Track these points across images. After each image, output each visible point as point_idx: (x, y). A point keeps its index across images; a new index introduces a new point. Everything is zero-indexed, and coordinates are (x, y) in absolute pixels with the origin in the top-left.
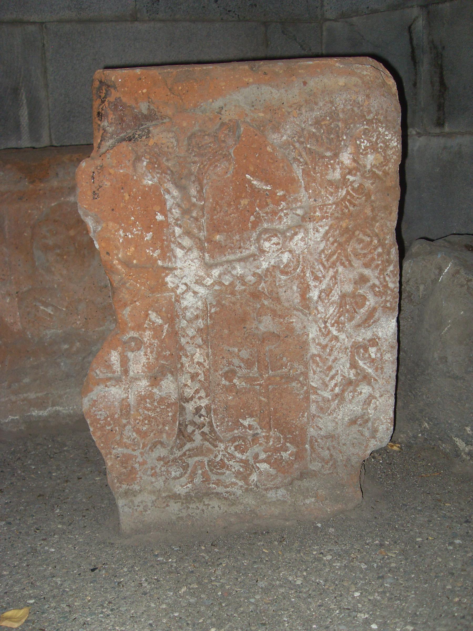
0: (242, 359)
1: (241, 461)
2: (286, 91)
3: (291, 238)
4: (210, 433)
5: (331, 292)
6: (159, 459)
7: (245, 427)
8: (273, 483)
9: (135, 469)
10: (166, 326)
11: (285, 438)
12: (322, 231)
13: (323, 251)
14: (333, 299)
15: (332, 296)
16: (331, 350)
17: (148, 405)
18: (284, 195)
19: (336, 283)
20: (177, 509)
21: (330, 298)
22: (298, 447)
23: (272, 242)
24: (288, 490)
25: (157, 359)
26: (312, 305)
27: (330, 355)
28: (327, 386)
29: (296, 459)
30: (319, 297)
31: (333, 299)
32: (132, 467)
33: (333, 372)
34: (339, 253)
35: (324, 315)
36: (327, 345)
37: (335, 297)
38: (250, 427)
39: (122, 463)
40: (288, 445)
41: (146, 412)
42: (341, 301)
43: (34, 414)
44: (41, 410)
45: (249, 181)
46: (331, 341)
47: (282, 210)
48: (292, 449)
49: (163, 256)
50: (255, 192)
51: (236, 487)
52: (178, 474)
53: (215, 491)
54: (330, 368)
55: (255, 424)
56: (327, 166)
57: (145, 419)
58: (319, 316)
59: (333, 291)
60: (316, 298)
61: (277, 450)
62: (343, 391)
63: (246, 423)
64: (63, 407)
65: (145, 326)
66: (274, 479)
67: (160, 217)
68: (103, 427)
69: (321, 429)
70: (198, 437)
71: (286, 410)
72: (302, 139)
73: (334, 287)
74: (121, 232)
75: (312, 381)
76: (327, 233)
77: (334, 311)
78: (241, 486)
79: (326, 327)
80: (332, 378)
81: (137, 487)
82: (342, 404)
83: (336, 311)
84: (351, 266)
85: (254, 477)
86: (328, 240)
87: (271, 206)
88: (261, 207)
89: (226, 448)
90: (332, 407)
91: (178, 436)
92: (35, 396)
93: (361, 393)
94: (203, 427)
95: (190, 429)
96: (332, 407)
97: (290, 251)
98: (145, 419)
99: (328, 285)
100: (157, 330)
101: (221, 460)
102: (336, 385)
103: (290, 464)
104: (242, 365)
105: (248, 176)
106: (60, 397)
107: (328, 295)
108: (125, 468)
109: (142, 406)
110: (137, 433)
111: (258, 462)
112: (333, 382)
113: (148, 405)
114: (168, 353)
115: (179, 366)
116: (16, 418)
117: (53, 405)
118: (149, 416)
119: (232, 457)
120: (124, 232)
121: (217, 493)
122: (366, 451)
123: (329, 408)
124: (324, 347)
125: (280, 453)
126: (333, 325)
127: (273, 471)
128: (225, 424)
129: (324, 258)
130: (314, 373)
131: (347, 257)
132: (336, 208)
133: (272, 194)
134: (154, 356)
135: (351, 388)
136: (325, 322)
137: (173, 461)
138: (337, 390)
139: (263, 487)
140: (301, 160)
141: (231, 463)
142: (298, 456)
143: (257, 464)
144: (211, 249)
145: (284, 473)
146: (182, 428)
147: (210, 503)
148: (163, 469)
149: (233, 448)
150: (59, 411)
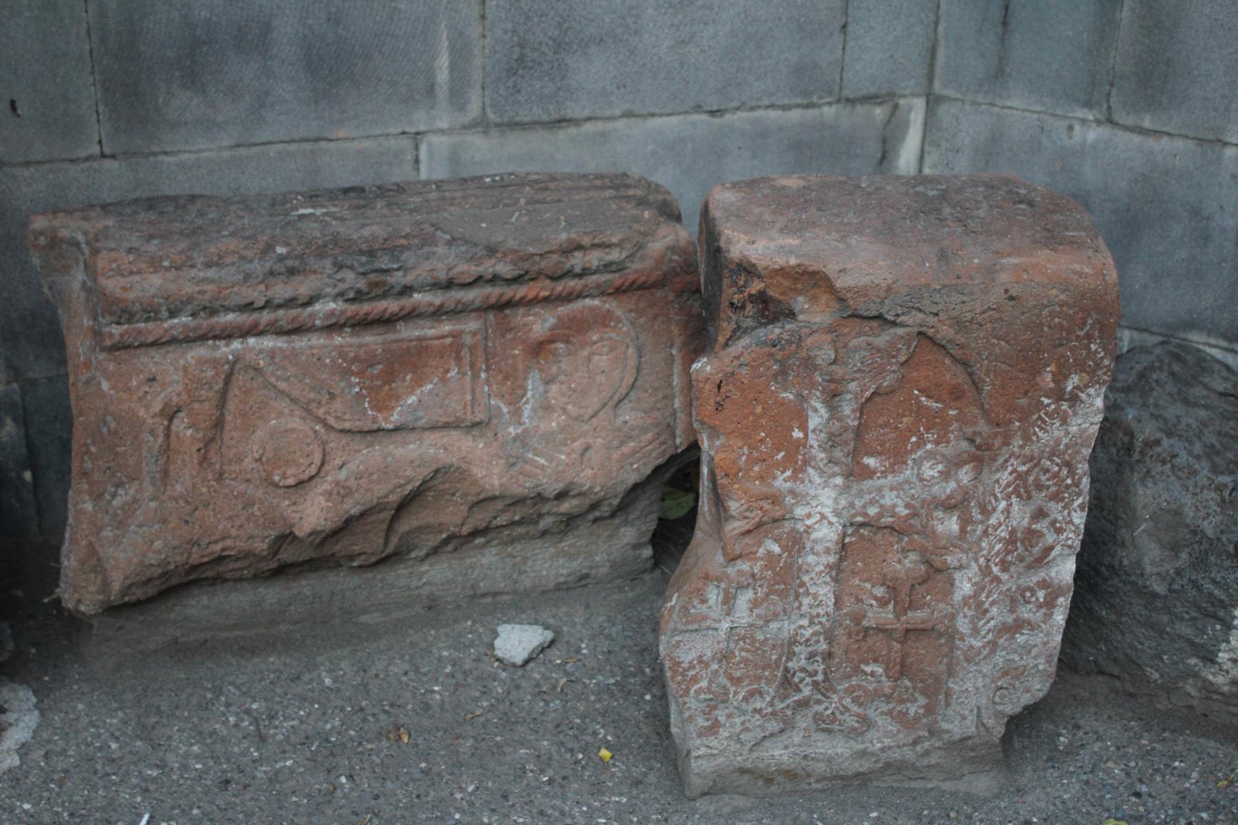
0: (876, 598)
1: (858, 715)
7: (865, 673)
38: (873, 674)
46: (991, 582)
48: (922, 701)
55: (879, 670)
61: (902, 701)
63: (868, 669)
67: (797, 434)
68: (685, 670)
74: (746, 449)
84: (1029, 498)
102: (989, 631)
103: (917, 719)
104: (874, 602)
115: (797, 604)
126: (996, 565)
130: (965, 616)
131: (1025, 487)
138: (990, 636)
142: (929, 710)
144: (856, 473)
149: (849, 700)
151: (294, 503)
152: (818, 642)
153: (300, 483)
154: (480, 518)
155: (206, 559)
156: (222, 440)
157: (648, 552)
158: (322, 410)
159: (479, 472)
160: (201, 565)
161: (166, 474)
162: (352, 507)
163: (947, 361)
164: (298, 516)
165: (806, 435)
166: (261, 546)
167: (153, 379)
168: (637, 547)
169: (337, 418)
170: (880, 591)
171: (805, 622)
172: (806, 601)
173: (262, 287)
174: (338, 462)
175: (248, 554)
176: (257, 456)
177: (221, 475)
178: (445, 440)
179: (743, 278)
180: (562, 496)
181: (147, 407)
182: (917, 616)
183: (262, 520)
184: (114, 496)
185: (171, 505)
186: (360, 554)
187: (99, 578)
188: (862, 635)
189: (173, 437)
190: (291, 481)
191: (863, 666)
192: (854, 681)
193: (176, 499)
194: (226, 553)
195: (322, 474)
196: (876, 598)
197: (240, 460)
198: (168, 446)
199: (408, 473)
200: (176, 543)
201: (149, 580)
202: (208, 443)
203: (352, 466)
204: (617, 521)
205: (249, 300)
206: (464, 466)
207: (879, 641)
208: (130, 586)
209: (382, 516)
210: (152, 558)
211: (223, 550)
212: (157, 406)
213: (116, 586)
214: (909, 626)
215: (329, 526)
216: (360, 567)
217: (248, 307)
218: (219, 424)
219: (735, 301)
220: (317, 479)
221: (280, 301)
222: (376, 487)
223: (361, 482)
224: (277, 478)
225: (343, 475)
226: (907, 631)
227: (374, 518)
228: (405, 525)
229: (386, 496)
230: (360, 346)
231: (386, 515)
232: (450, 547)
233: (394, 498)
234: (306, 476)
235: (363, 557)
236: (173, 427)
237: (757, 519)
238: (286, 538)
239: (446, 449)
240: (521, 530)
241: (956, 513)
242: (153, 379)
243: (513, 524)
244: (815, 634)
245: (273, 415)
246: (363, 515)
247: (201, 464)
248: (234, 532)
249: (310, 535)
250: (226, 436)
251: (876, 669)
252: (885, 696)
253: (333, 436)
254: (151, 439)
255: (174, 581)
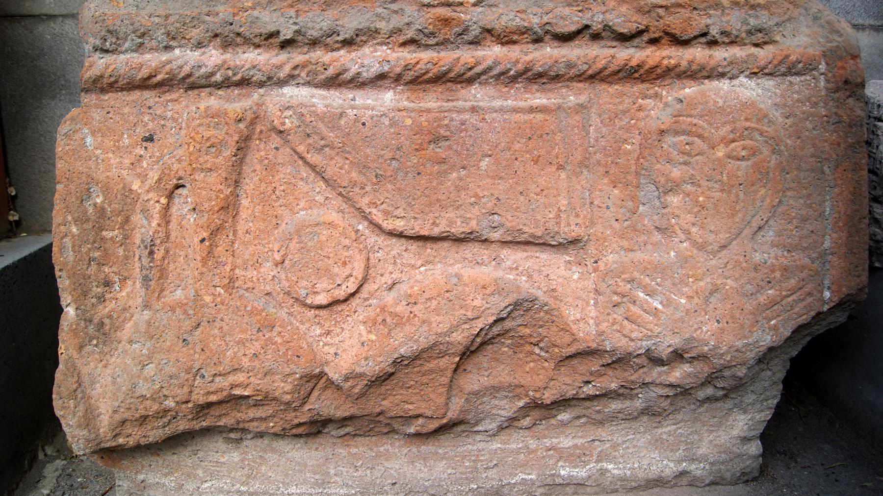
43: (562, 472)
44: (574, 467)
64: (615, 464)
92: (571, 444)
106: (615, 446)
116: (530, 477)
117: (597, 462)
150: (607, 470)
151: (328, 333)
153: (336, 302)
154: (567, 383)
155: (213, 398)
156: (235, 233)
157: (755, 448)
158: (366, 200)
159: (572, 314)
160: (210, 405)
161: (163, 273)
162: (403, 343)
164: (332, 351)
166: (282, 387)
167: (150, 139)
168: (745, 440)
169: (386, 213)
173: (292, 12)
174: (388, 279)
175: (266, 399)
176: (278, 257)
177: (232, 280)
178: (529, 264)
180: (678, 356)
181: (143, 177)
183: (283, 350)
184: (101, 299)
185: (164, 318)
186: (417, 416)
187: (81, 408)
189: (173, 226)
190: (322, 299)
193: (173, 310)
194: (237, 392)
195: (364, 293)
197: (257, 265)
198: (168, 237)
199: (477, 303)
200: (170, 369)
201: (144, 420)
202: (215, 232)
203: (404, 288)
204: (729, 404)
205: (273, 29)
206: (551, 301)
208: (124, 422)
209: (443, 362)
210: (144, 389)
211: (233, 386)
212: (154, 176)
213: (104, 423)
215: (371, 368)
216: (418, 435)
217: (268, 38)
218: (229, 207)
220: (355, 302)
221: (315, 34)
222: (434, 319)
223: (415, 309)
224: (303, 292)
225: (389, 298)
227: (432, 365)
228: (474, 380)
229: (446, 334)
230: (421, 111)
231: (448, 362)
232: (526, 422)
233: (460, 338)
234: (341, 293)
235: (421, 421)
236: (174, 210)
238: (316, 379)
239: (530, 276)
240: (615, 405)
242: (150, 139)
243: (606, 395)
245: (302, 204)
246: (416, 358)
247: (204, 261)
248: (245, 362)
249: (347, 379)
250: (241, 227)
253: (381, 240)
254: (145, 222)
255: (182, 426)
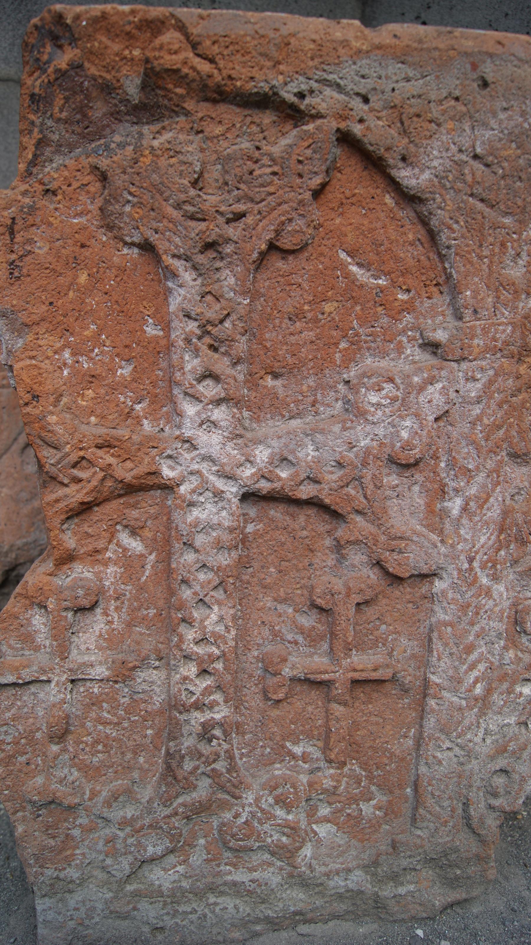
0: (301, 630)
2: (437, 77)
3: (421, 389)
4: (229, 771)
5: (486, 500)
6: (123, 823)
7: (294, 757)
8: (341, 860)
9: (73, 838)
10: (153, 557)
11: (370, 778)
12: (483, 378)
13: (479, 418)
14: (489, 514)
15: (488, 509)
16: (477, 613)
17: (105, 714)
18: (411, 301)
19: (498, 483)
20: (152, 914)
21: (484, 512)
22: (391, 792)
23: (384, 392)
24: (367, 873)
25: (129, 625)
26: (448, 526)
27: (472, 624)
28: (460, 682)
29: (386, 814)
30: (465, 509)
31: (489, 514)
32: (67, 835)
33: (473, 657)
34: (511, 425)
35: (470, 546)
36: (469, 605)
37: (494, 512)
38: (305, 758)
39: (48, 828)
40: (373, 788)
41: (101, 727)
42: (504, 519)
45: (343, 266)
47: (404, 331)
48: (380, 798)
49: (152, 414)
50: (353, 292)
51: (271, 869)
52: (159, 850)
53: (229, 878)
54: (470, 649)
56: (503, 245)
57: (97, 742)
58: (460, 547)
59: (492, 500)
60: (455, 512)
61: (354, 800)
62: (489, 691)
63: (298, 750)
65: (109, 554)
66: (343, 852)
67: (151, 330)
69: (440, 763)
70: (204, 784)
71: (377, 724)
72: (459, 185)
73: (493, 490)
74: (67, 354)
75: (433, 673)
76: (491, 382)
77: (489, 539)
78: (281, 869)
79: (471, 569)
80: (473, 667)
81: (73, 873)
82: (485, 714)
83: (493, 537)
85: (307, 851)
86: (491, 397)
87: (385, 320)
88: (363, 321)
89: (257, 800)
90: (466, 722)
91: (163, 777)
93: (521, 694)
94: (214, 761)
95: (188, 765)
96: (466, 722)
97: (417, 415)
98: (97, 742)
99: (484, 486)
100: (130, 564)
101: (246, 823)
103: (375, 825)
104: (300, 639)
105: (343, 255)
107: (481, 507)
108: (54, 837)
109: (93, 715)
110: (79, 770)
111: (316, 822)
112: (475, 673)
113: (105, 714)
114: (152, 612)
118: (107, 737)
119: (269, 816)
120: (73, 354)
121: (235, 884)
122: (517, 798)
123: (460, 723)
124: (464, 608)
125: (358, 805)
127: (341, 839)
128: (258, 751)
129: (481, 432)
132: (513, 332)
133: (382, 299)
134: (124, 616)
135: (505, 686)
136: (471, 560)
137: (151, 826)
139: (323, 869)
140: (455, 226)
141: (266, 827)
143: (314, 826)
145: (361, 841)
146: (174, 764)
147: (220, 900)
148: (130, 841)
149: (271, 800)
152: (211, 706)
163: (389, 200)
165: (167, 328)
170: (307, 621)
171: (192, 670)
172: (190, 635)
179: (49, 48)
182: (363, 661)
188: (284, 690)
191: (288, 744)
192: (279, 770)
196: (301, 630)
207: (309, 703)
214: (357, 676)
219: (37, 91)
226: (355, 682)
237: (94, 483)
241: (419, 477)
244: (207, 691)
251: (310, 749)
252: (325, 791)
